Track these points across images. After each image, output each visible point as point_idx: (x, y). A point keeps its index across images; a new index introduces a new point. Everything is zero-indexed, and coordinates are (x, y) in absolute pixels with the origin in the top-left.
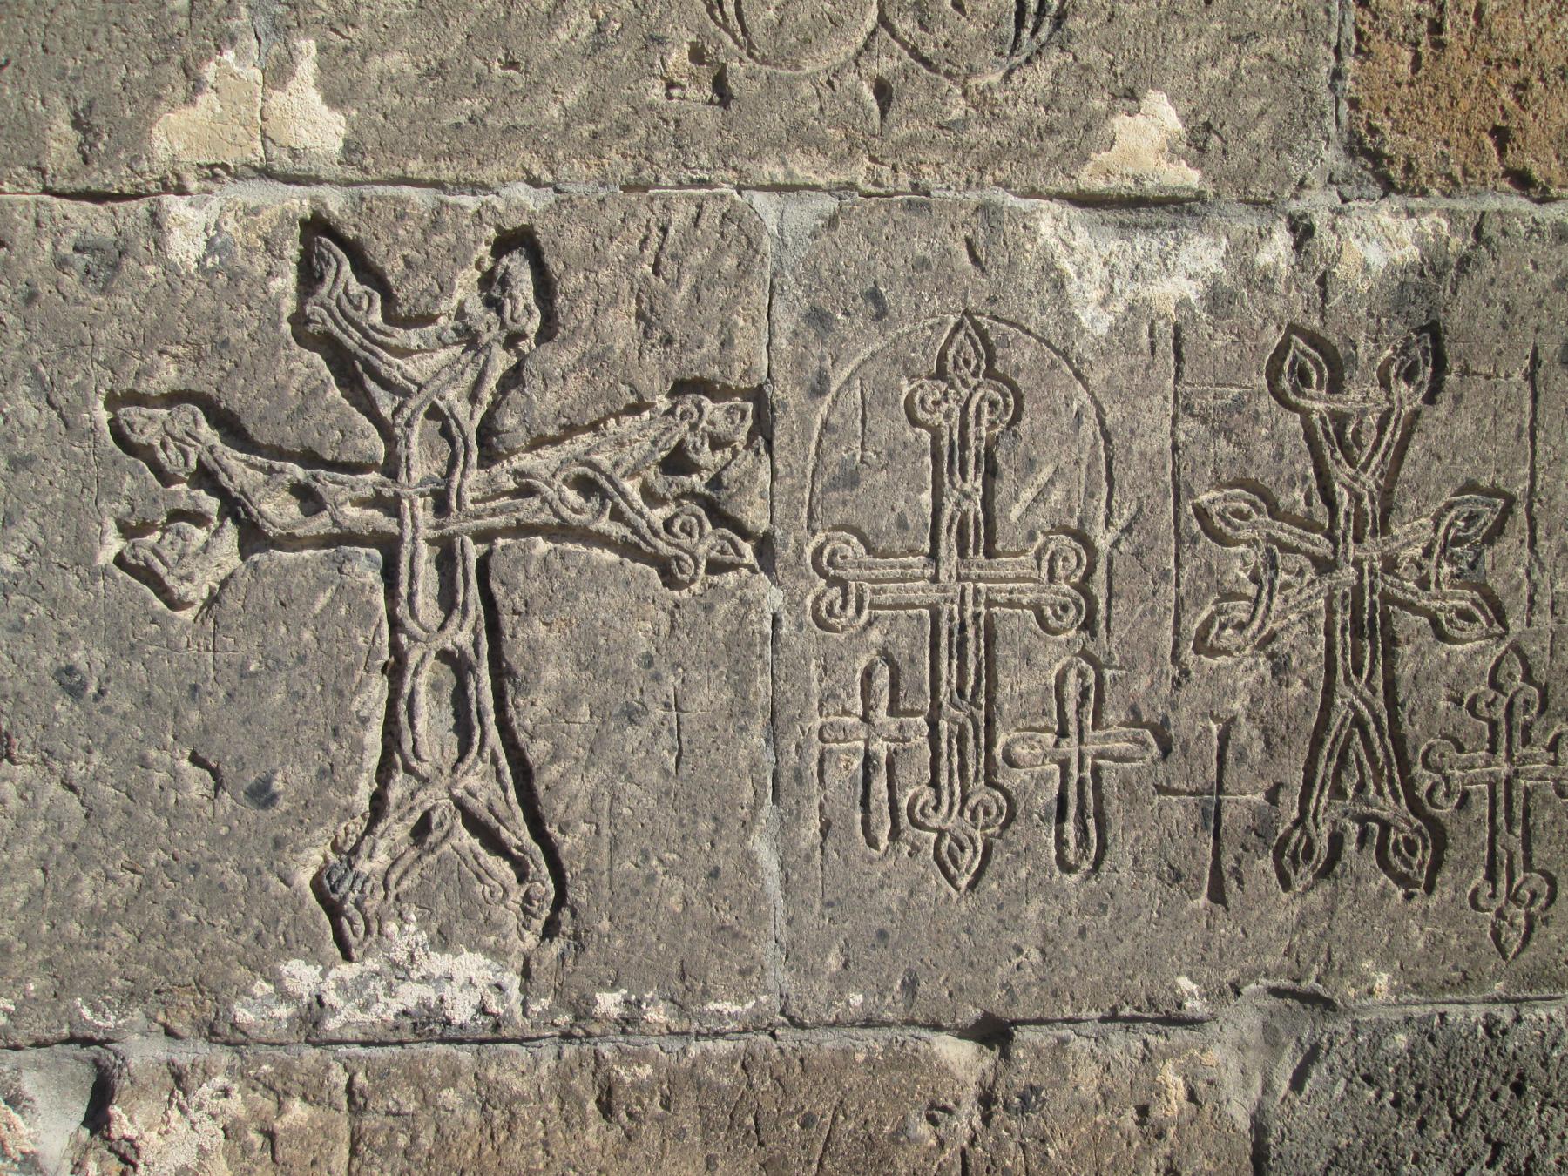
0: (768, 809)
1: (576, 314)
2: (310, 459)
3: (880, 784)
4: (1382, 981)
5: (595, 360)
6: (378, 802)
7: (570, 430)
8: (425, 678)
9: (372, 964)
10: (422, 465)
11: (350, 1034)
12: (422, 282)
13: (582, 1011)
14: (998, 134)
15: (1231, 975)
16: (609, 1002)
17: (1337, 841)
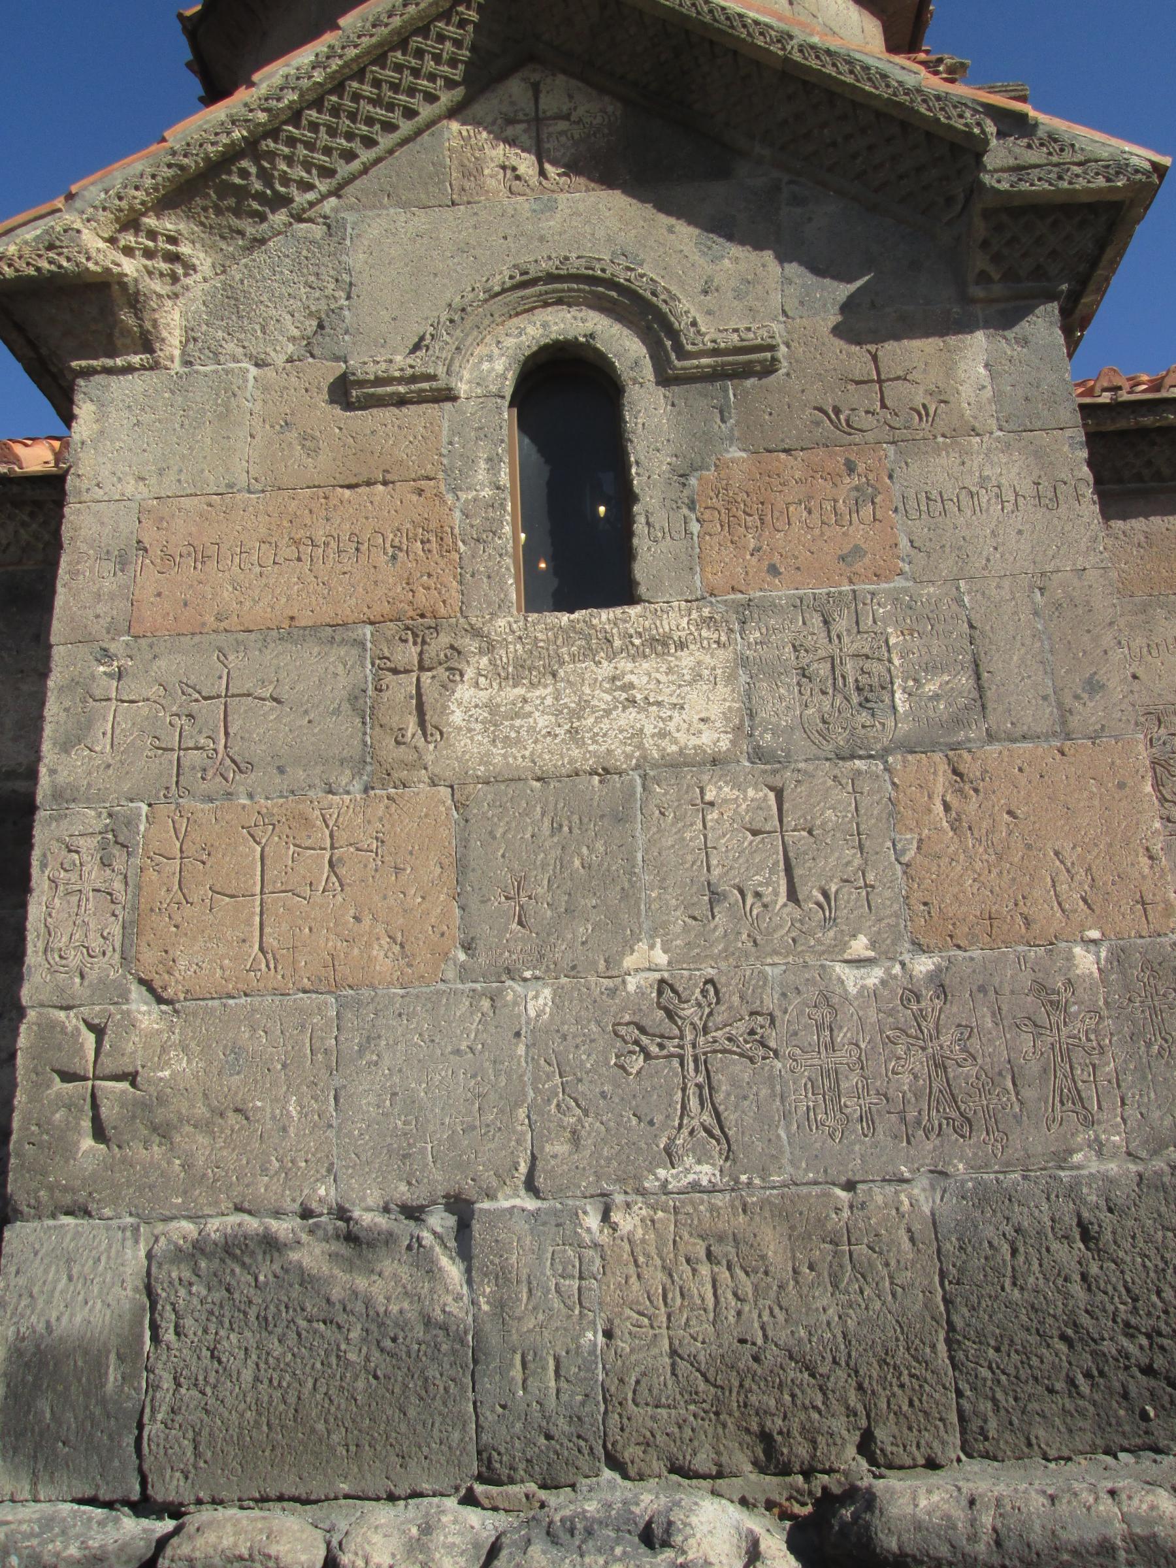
0: (782, 1122)
1: (725, 997)
2: (662, 1036)
3: (812, 1114)
4: (961, 1166)
5: (730, 1008)
6: (681, 1126)
7: (725, 1026)
8: (692, 1091)
9: (681, 1169)
10: (689, 1037)
11: (675, 1190)
12: (688, 992)
13: (737, 1181)
14: (823, 948)
15: (916, 1165)
16: (744, 1178)
17: (940, 1125)
